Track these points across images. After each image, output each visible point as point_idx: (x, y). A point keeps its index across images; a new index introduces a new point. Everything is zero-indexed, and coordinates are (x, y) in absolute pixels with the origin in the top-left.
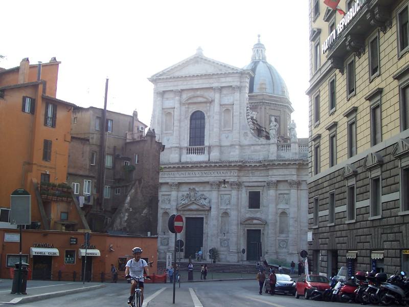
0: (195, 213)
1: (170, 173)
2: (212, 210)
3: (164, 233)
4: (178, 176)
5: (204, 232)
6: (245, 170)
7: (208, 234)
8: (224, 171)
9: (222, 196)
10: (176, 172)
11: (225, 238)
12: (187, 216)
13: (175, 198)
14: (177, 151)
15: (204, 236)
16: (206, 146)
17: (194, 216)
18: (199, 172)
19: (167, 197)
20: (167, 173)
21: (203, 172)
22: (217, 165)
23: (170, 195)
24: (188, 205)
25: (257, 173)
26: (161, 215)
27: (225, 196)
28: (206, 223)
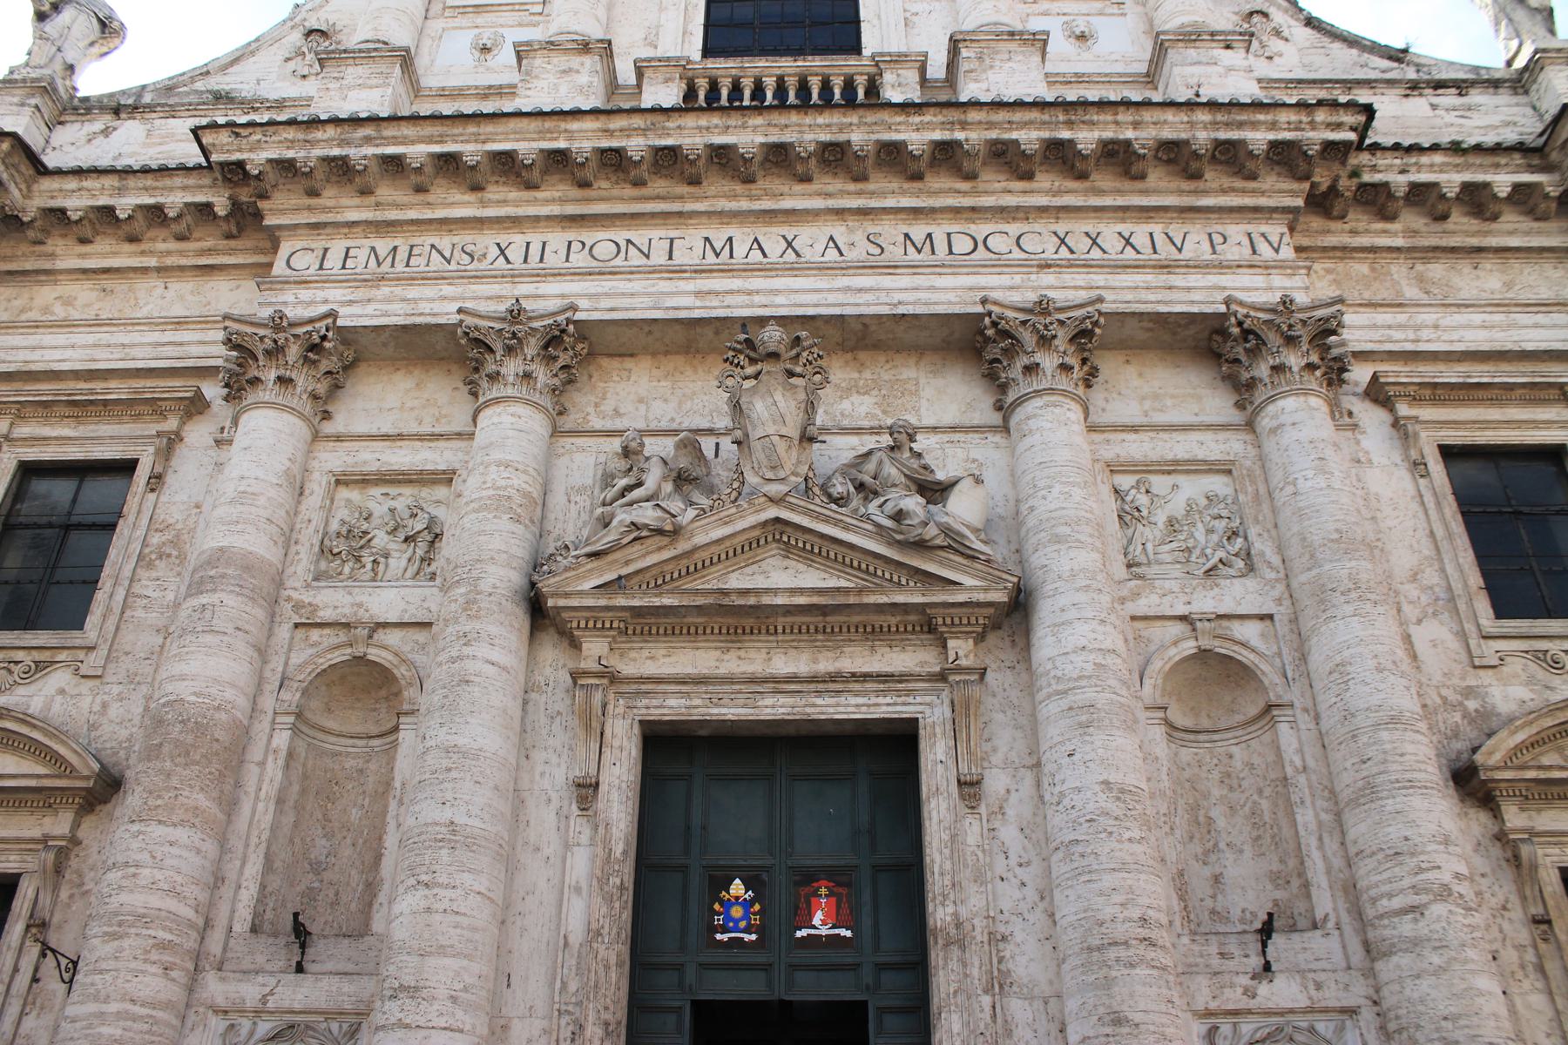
0: (785, 663)
1: (486, 242)
2: (1046, 612)
3: (301, 933)
4: (579, 260)
5: (939, 914)
6: (1345, 252)
7: (997, 939)
8: (1140, 232)
9: (1125, 482)
10: (557, 239)
11: (1282, 992)
12: (673, 707)
13: (518, 481)
14: (584, 79)
15: (945, 978)
16: (899, 59)
17: (774, 708)
18: (839, 231)
19: (404, 497)
20: (445, 243)
21: (891, 231)
22: (1086, 138)
23: (446, 478)
24: (693, 563)
25: (1488, 280)
26: (291, 697)
27: (1159, 483)
28: (970, 788)
